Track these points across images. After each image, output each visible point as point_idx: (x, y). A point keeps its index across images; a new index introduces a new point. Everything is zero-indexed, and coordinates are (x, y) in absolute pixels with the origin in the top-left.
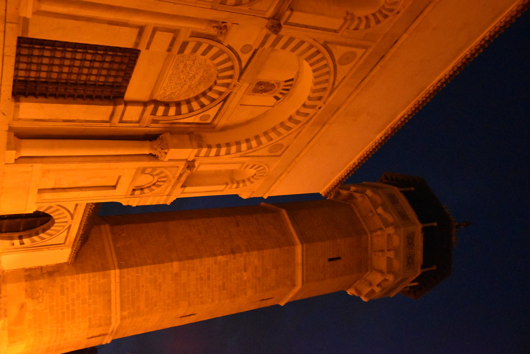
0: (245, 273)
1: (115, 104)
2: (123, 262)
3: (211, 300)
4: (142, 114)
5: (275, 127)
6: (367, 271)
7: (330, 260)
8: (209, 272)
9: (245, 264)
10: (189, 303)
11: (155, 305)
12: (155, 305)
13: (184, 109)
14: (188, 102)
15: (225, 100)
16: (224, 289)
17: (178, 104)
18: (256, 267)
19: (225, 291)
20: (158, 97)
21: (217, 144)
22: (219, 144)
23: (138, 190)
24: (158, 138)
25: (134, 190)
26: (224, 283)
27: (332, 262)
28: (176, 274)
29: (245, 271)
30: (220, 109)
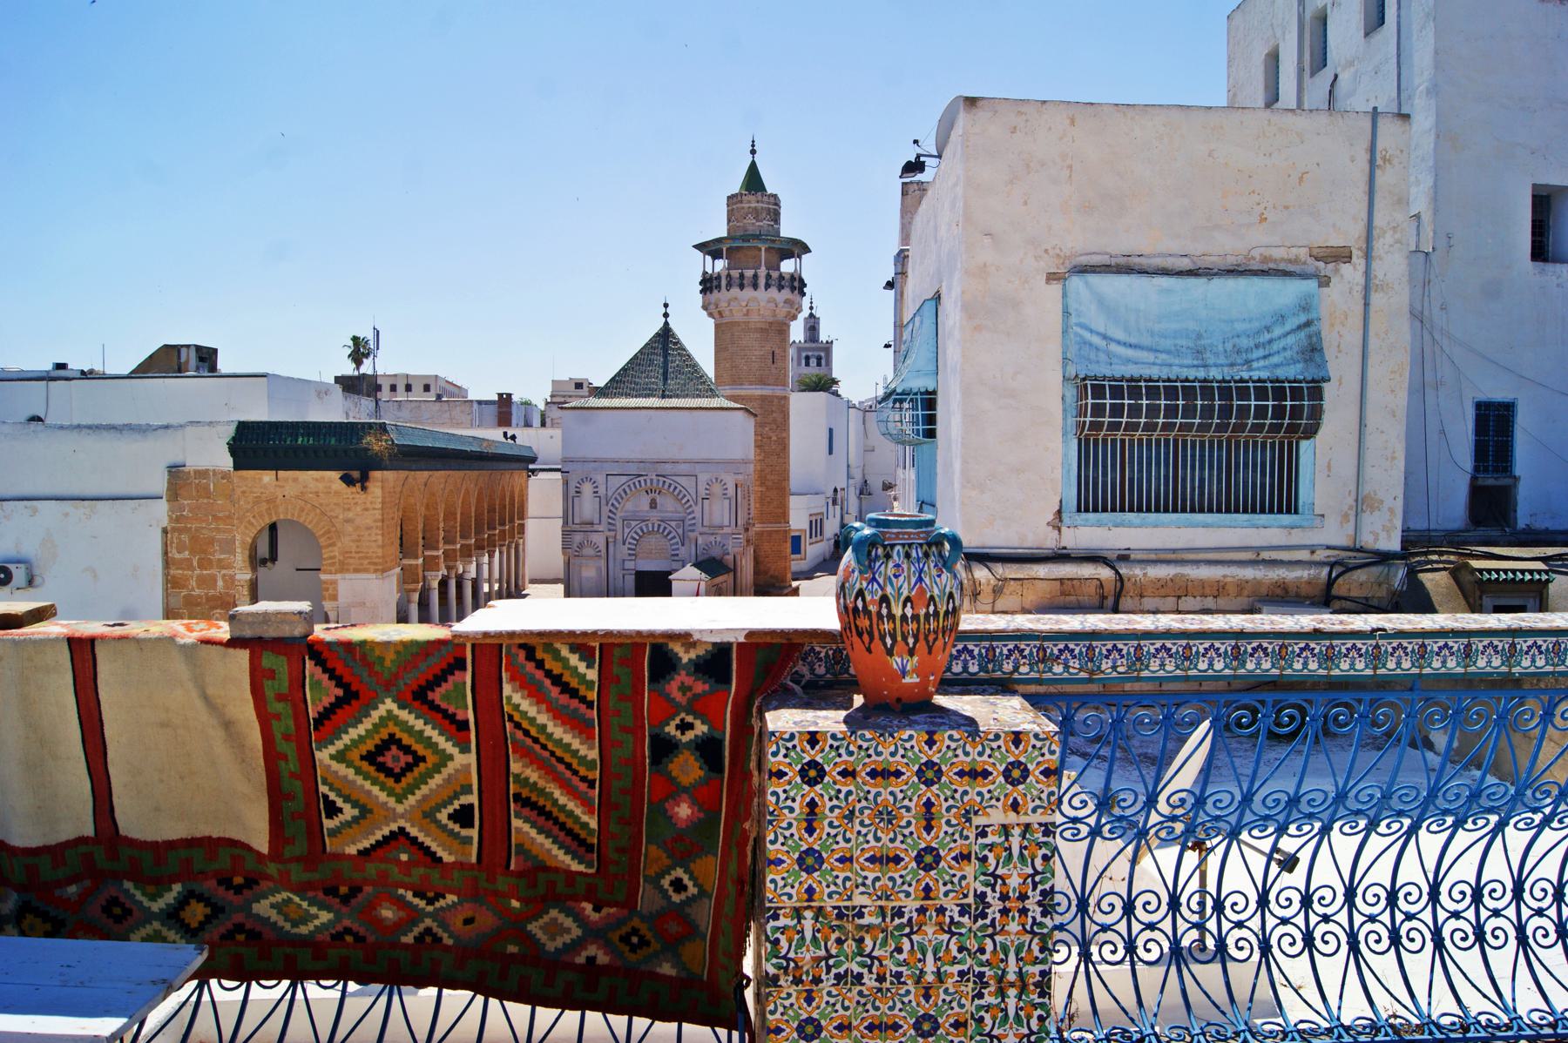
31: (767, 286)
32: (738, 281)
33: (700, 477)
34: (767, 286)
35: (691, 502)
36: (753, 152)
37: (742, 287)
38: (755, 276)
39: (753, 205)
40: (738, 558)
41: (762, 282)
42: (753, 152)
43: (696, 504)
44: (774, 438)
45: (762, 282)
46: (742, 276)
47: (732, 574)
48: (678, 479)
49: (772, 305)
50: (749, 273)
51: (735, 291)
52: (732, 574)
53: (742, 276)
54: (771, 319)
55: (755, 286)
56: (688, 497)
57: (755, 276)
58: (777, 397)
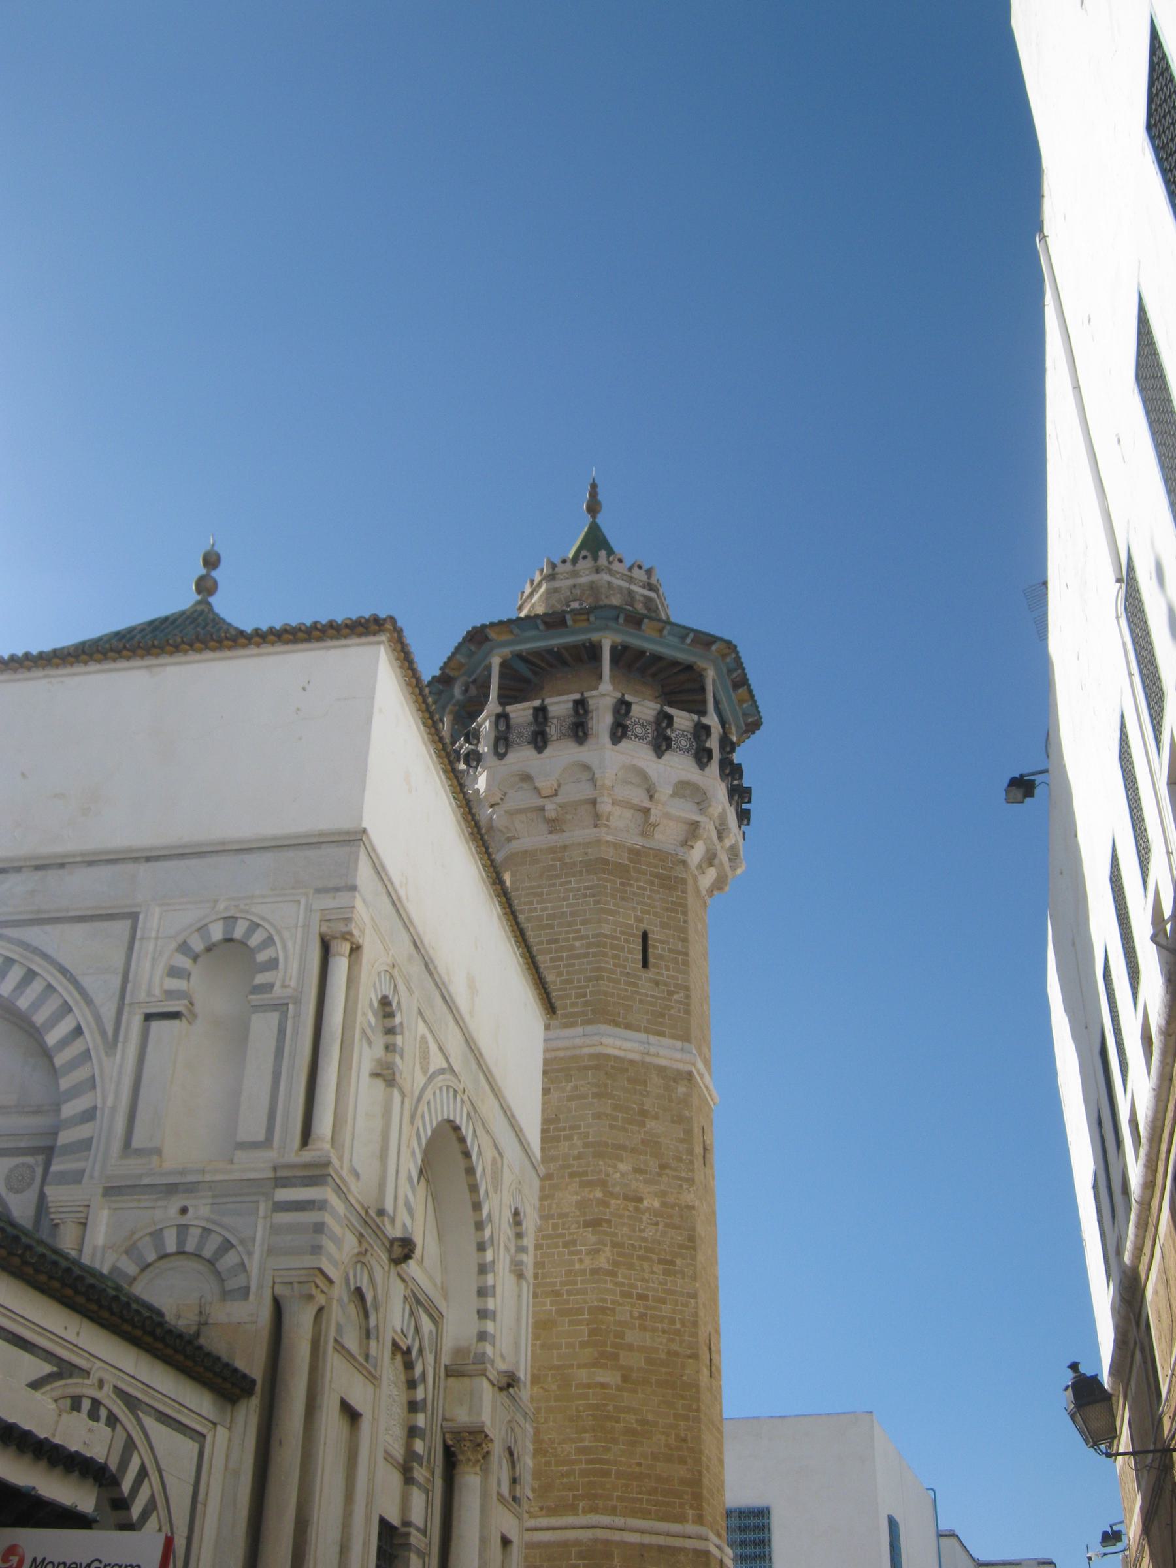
0: (646, 1203)
1: (407, 1546)
2: (581, 1505)
3: (692, 1301)
4: (420, 1486)
5: (469, 1185)
6: (684, 863)
7: (645, 964)
8: (628, 1295)
9: (626, 1198)
10: (689, 1357)
11: (685, 1440)
12: (685, 1440)
13: (420, 1394)
14: (412, 1384)
15: (418, 1302)
16: (672, 1263)
17: (413, 1407)
18: (638, 1170)
19: (678, 1261)
20: (398, 1452)
21: (475, 1316)
22: (478, 1312)
23: (515, 1489)
24: (453, 1449)
25: (514, 1499)
26: (660, 1261)
27: (652, 960)
28: (625, 1379)
29: (640, 1200)
30: (426, 1310)
31: (619, 732)
32: (528, 732)
33: (153, 921)
34: (619, 732)
35: (90, 1037)
36: (594, 508)
37: (540, 740)
38: (581, 706)
39: (583, 580)
40: (301, 1324)
41: (602, 720)
42: (594, 508)
43: (111, 1044)
44: (651, 1202)
45: (602, 720)
46: (541, 713)
47: (249, 1413)
48: (34, 935)
49: (638, 796)
50: (560, 706)
51: (522, 757)
52: (249, 1413)
53: (541, 713)
54: (637, 841)
55: (579, 730)
56: (81, 1014)
57: (581, 706)
58: (661, 1070)
